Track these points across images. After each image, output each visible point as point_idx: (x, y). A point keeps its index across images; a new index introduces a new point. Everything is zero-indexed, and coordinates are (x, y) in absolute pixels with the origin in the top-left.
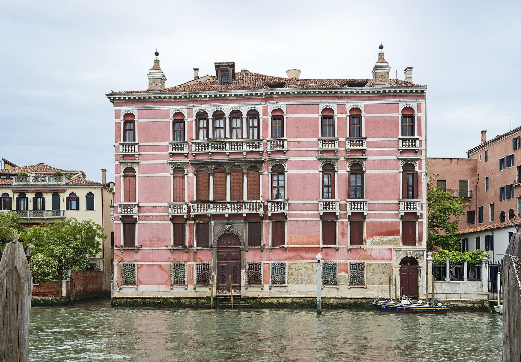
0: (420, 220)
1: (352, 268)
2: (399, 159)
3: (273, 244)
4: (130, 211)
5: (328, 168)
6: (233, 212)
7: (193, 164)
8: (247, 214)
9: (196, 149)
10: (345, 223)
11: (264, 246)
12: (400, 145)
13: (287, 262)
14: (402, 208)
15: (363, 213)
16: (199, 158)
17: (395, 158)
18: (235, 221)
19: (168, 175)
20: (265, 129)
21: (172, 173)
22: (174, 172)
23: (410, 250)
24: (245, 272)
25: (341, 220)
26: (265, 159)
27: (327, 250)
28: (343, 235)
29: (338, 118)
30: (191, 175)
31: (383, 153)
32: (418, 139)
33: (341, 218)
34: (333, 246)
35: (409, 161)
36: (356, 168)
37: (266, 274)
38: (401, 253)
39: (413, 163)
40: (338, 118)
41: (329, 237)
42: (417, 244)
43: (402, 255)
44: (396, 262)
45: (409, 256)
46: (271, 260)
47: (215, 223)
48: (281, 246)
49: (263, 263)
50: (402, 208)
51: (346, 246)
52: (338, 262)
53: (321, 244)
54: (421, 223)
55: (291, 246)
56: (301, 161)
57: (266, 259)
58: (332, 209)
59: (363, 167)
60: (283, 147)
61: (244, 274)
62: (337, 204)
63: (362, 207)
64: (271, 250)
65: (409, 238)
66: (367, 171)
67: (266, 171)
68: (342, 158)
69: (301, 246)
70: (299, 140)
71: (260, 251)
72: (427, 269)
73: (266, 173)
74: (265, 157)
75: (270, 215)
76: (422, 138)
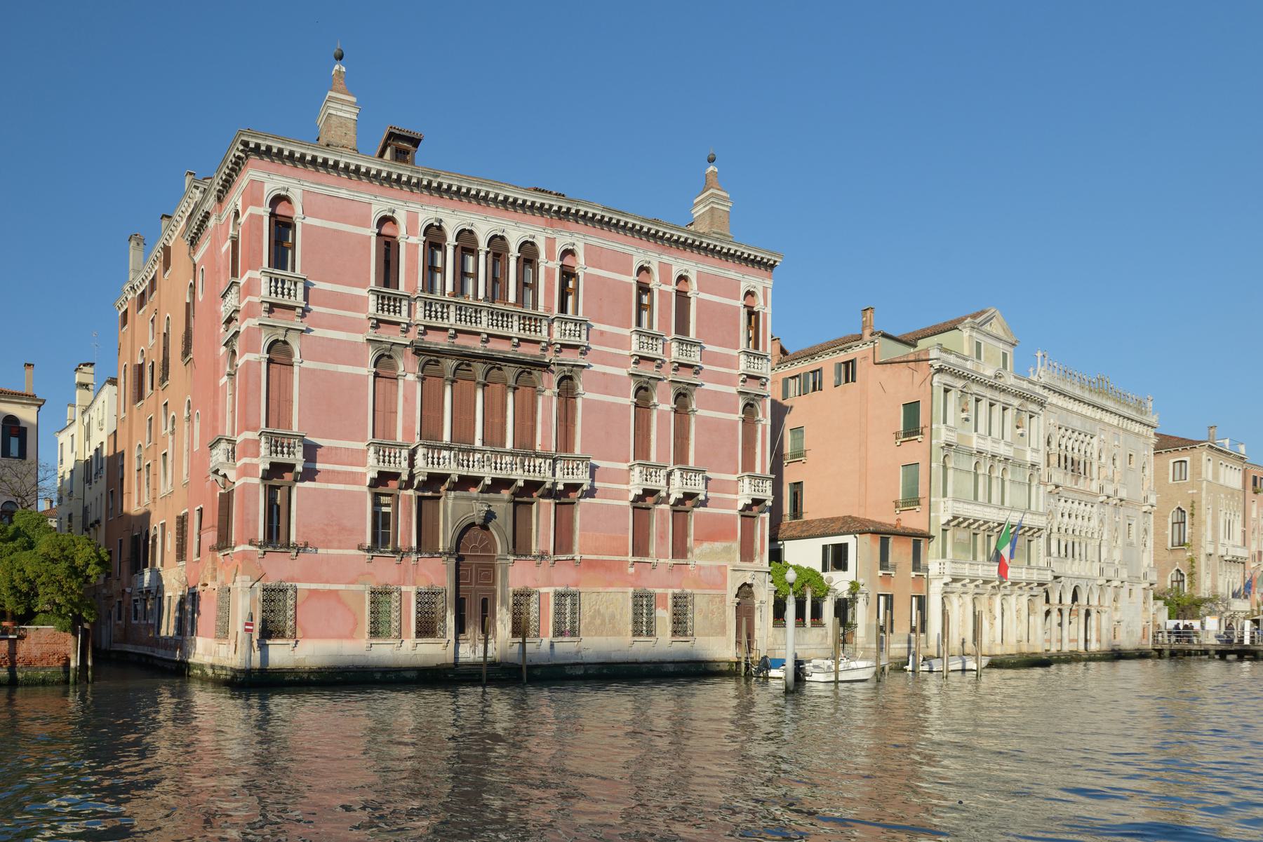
2: (741, 393)
7: (419, 351)
30: (411, 377)
42: (757, 560)
48: (570, 557)
52: (658, 591)
55: (585, 557)
56: (604, 374)
67: (549, 386)
69: (601, 557)
74: (549, 357)
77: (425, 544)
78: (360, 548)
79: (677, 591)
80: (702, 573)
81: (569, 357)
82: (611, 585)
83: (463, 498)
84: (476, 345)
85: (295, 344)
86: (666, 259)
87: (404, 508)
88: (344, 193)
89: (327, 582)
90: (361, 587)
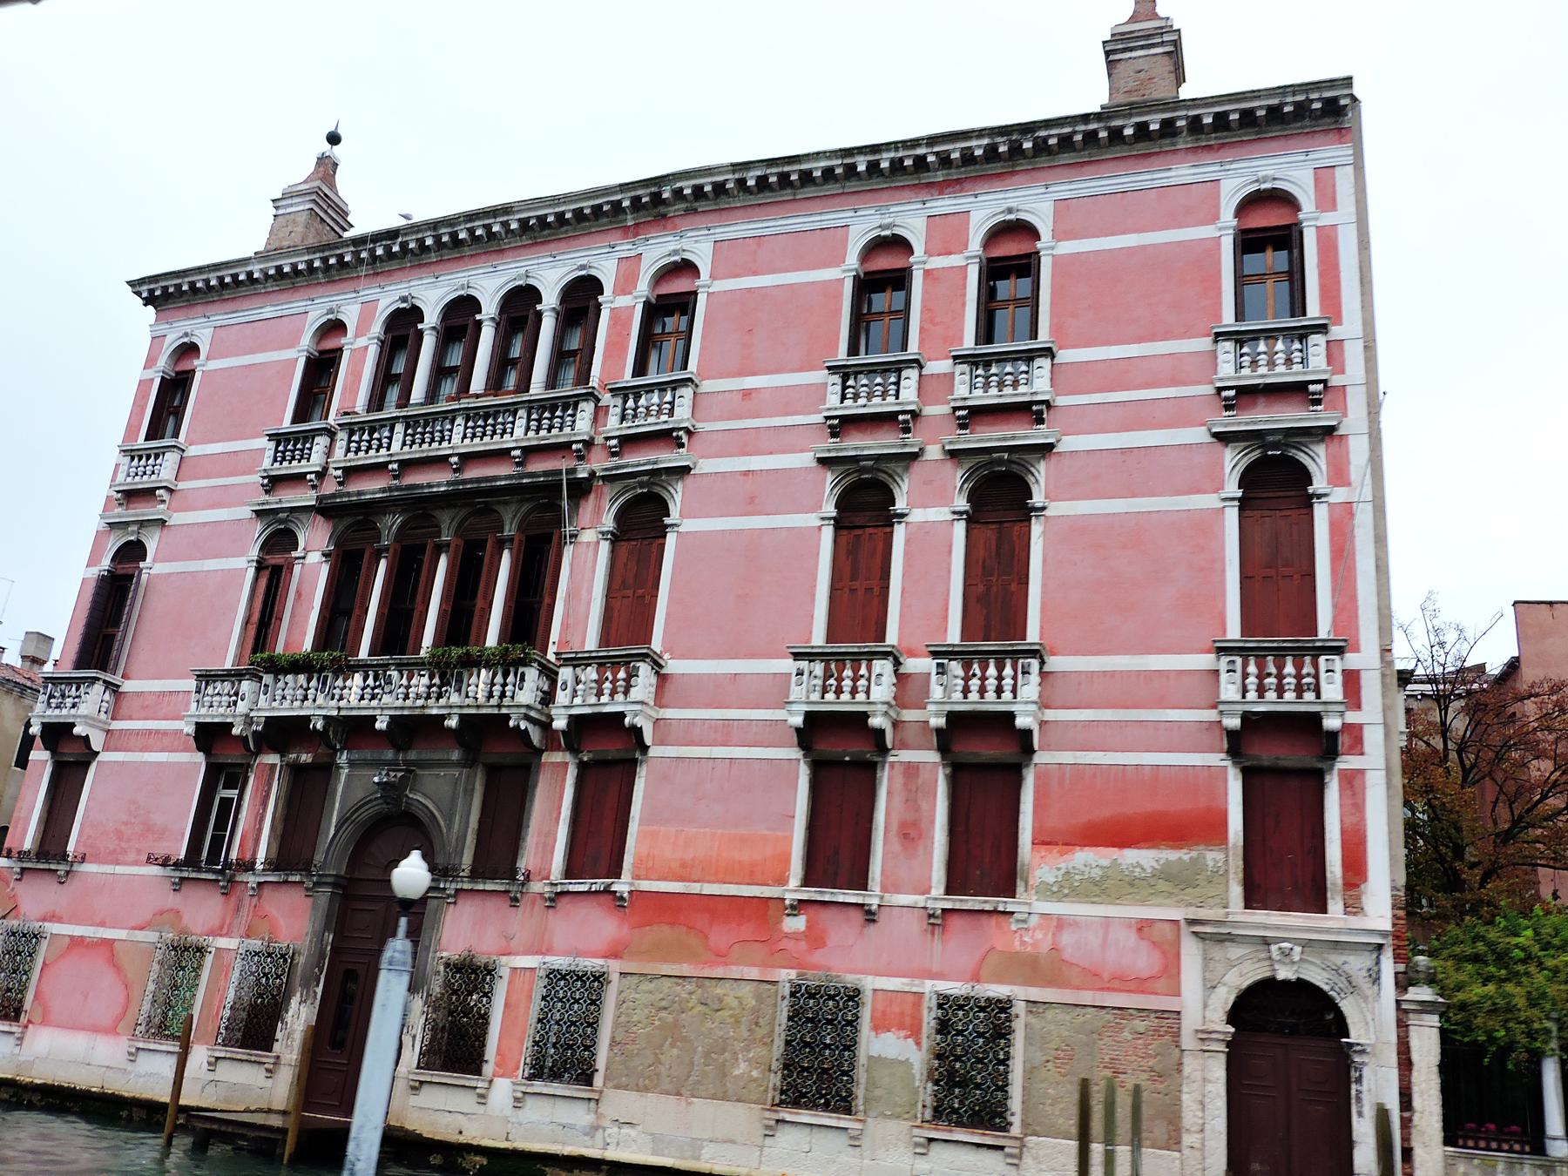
0: (1346, 762)
1: (943, 1027)
2: (1223, 438)
3: (570, 872)
4: (74, 706)
5: (865, 503)
7: (325, 509)
10: (924, 775)
11: (528, 878)
13: (614, 967)
14: (1229, 690)
15: (1011, 716)
18: (428, 755)
20: (615, 347)
21: (254, 553)
23: (1290, 944)
25: (905, 756)
26: (592, 474)
27: (825, 915)
28: (911, 834)
29: (927, 273)
30: (315, 557)
32: (1322, 329)
33: (904, 746)
34: (851, 896)
35: (1275, 446)
36: (1000, 495)
37: (509, 1023)
38: (1235, 952)
39: (1302, 457)
40: (927, 273)
41: (838, 851)
42: (1335, 905)
43: (1244, 972)
45: (1284, 974)
47: (352, 764)
48: (599, 884)
49: (506, 964)
50: (1229, 690)
51: (920, 900)
52: (869, 983)
53: (795, 879)
54: (1353, 781)
55: (645, 885)
56: (746, 473)
57: (521, 946)
60: (671, 413)
63: (1008, 682)
65: (1286, 865)
66: (1056, 509)
68: (933, 452)
69: (695, 888)
70: (750, 382)
71: (502, 904)
72: (1405, 1063)
73: (588, 536)
75: (560, 724)
76: (1348, 328)
77: (291, 855)
79: (955, 988)
80: (1067, 939)
81: (639, 460)
82: (721, 956)
83: (367, 764)
85: (151, 547)
86: (944, 204)
87: (255, 791)
88: (268, 312)
89: (102, 924)
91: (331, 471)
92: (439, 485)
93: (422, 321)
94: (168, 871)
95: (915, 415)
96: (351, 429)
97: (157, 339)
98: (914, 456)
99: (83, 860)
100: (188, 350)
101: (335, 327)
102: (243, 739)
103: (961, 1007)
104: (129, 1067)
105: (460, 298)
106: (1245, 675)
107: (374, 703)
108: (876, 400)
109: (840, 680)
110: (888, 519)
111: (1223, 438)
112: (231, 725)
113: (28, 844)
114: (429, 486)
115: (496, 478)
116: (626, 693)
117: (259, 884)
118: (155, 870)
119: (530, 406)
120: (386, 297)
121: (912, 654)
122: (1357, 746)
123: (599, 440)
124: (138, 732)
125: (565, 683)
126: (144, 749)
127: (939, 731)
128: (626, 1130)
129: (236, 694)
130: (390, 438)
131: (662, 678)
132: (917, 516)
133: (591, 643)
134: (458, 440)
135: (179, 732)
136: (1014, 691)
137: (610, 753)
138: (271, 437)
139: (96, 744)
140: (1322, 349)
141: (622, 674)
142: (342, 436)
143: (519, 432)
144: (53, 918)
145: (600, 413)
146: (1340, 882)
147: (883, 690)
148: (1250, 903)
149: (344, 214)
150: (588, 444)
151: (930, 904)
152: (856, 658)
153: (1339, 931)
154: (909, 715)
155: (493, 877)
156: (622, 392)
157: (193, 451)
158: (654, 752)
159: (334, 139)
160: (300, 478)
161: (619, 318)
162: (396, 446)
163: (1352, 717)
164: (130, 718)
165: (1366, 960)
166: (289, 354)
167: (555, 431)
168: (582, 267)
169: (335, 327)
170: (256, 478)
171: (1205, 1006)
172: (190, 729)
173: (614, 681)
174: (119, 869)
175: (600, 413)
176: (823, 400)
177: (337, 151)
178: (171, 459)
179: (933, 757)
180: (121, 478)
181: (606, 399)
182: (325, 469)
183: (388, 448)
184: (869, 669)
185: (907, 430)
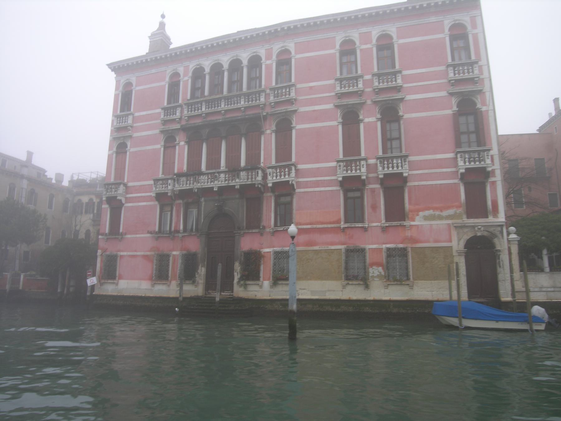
0: (492, 179)
2: (451, 94)
3: (276, 225)
4: (115, 191)
6: (224, 184)
8: (240, 185)
9: (188, 111)
12: (451, 75)
14: (461, 163)
15: (402, 173)
16: (192, 122)
17: (444, 93)
19: (158, 146)
21: (163, 143)
22: (165, 142)
24: (240, 263)
26: (267, 113)
28: (374, 207)
29: (361, 50)
30: (182, 143)
31: (426, 89)
33: (370, 184)
40: (361, 50)
41: (354, 212)
44: (457, 244)
45: (479, 234)
46: (274, 247)
47: (205, 201)
50: (461, 163)
51: (379, 224)
53: (342, 223)
54: (494, 183)
58: (356, 170)
59: (400, 111)
60: (289, 95)
61: (237, 267)
62: (363, 163)
64: (274, 233)
66: (406, 116)
68: (369, 102)
72: (510, 254)
73: (268, 132)
78: (151, 233)
84: (219, 118)
85: (129, 144)
86: (364, 30)
88: (154, 71)
90: (153, 253)
91: (183, 117)
92: (220, 119)
93: (205, 71)
94: (153, 235)
95: (363, 91)
96: (188, 105)
97: (118, 82)
98: (364, 103)
99: (126, 234)
100: (128, 85)
101: (176, 75)
102: (171, 197)
103: (394, 251)
104: (153, 288)
105: (215, 64)
106: (465, 158)
107: (212, 183)
108: (351, 88)
109: (351, 167)
110: (358, 121)
111: (451, 94)
112: (167, 193)
113: (107, 231)
114: (216, 120)
115: (238, 116)
116: (289, 175)
117: (183, 236)
118: (149, 235)
119: (245, 95)
120: (192, 65)
121: (370, 159)
122: (494, 176)
123: (267, 104)
124: (135, 197)
125: (270, 173)
126: (139, 202)
127: (381, 179)
128: (303, 291)
129: (167, 184)
130: (201, 107)
131: (297, 170)
132: (366, 120)
133: (274, 163)
134: (223, 106)
135: (151, 196)
136: (402, 166)
137: (284, 191)
138: (162, 109)
139: (123, 201)
140: (477, 68)
141: (287, 170)
142: (184, 107)
143: (242, 103)
144: (119, 251)
145: (267, 96)
146: (491, 210)
147: (364, 170)
148: (468, 218)
149: (169, 39)
150: (265, 105)
151: (382, 225)
152: (356, 161)
153: (493, 222)
154: (371, 175)
155: (253, 228)
156: (273, 89)
157: (137, 114)
158: (298, 191)
159: (163, 16)
160: (173, 121)
161: (269, 67)
162: (204, 109)
163: (493, 168)
164: (132, 193)
165: (499, 229)
166: (163, 83)
167: (254, 102)
168: (254, 52)
169: (176, 75)
170: (159, 121)
171: (459, 244)
172: (153, 195)
173: (285, 172)
174: (138, 236)
175: (267, 96)
176: (335, 88)
177: (165, 20)
178: (130, 118)
179: (378, 186)
180: (115, 124)
181: (268, 91)
182: (181, 117)
183: (201, 109)
184: (360, 163)
185: (361, 96)
